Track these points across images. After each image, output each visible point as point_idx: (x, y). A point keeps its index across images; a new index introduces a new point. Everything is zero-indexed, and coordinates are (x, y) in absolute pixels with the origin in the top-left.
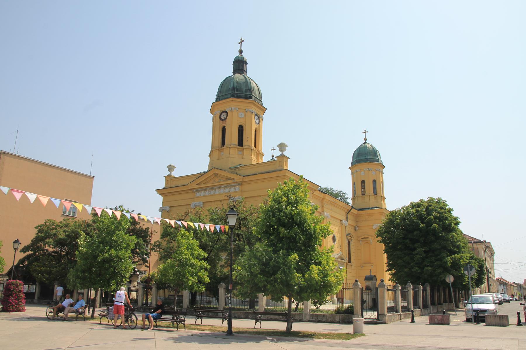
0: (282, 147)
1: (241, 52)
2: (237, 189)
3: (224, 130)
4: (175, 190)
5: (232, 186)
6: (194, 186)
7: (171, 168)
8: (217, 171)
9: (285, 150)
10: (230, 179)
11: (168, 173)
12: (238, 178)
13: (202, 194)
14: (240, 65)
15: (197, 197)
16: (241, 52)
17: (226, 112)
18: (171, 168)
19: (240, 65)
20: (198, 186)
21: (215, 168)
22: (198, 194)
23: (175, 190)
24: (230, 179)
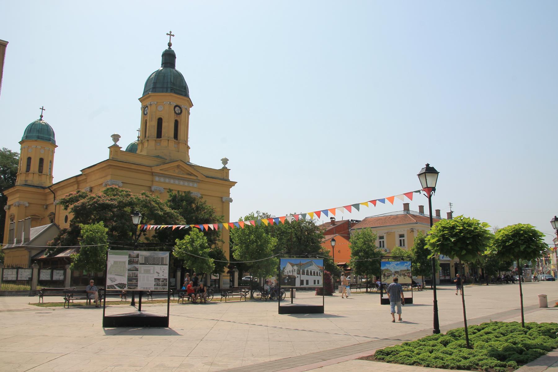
0: (225, 161)
1: (170, 45)
2: (195, 185)
3: (176, 123)
4: (133, 167)
5: (193, 181)
6: (157, 170)
7: (116, 138)
8: (181, 164)
9: (227, 163)
10: (191, 174)
11: (113, 143)
12: (200, 177)
13: (162, 180)
14: (169, 58)
15: (157, 182)
16: (170, 45)
17: (180, 108)
18: (116, 138)
19: (169, 58)
20: (161, 172)
21: (181, 161)
22: (157, 179)
23: (133, 167)
24: (191, 174)
